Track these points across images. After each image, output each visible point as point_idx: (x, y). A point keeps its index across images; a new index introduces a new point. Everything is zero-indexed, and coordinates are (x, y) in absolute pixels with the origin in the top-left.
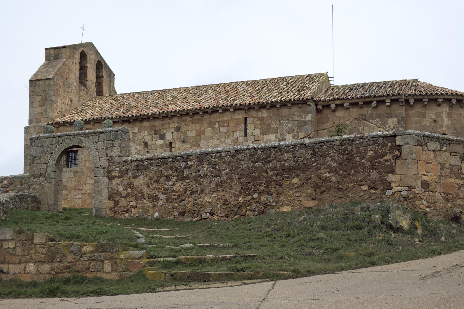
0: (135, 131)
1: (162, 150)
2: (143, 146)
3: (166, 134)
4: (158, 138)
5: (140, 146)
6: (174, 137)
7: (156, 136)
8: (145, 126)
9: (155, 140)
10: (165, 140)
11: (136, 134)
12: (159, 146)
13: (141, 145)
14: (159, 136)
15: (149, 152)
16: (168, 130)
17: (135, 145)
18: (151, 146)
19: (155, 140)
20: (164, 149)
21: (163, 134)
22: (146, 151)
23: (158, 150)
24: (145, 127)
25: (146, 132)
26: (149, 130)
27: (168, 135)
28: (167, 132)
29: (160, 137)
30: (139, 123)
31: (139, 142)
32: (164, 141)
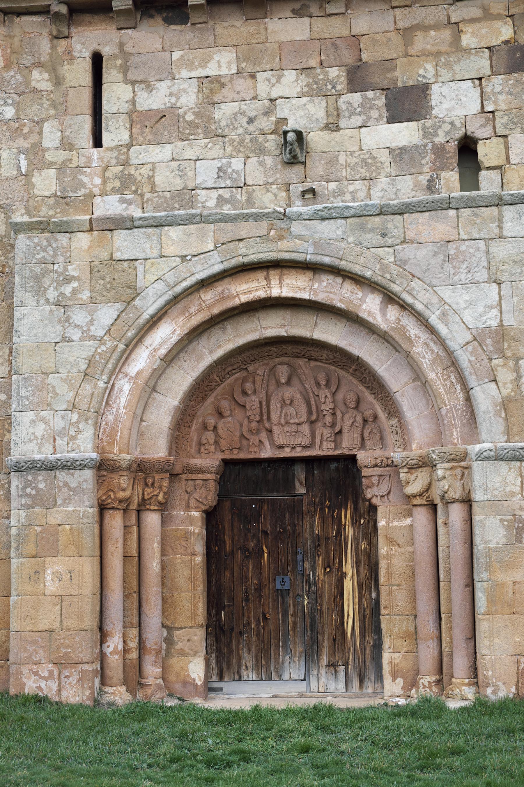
0: (211, 70)
1: (411, 184)
2: (269, 161)
3: (435, 88)
4: (375, 114)
5: (254, 160)
6: (495, 103)
7: (365, 98)
8: (284, 38)
9: (358, 120)
10: (429, 123)
11: (223, 85)
12: (385, 157)
13: (261, 151)
14: (382, 101)
15: (313, 191)
16: (448, 65)
17: (216, 151)
18: (333, 161)
19: (358, 120)
20: (423, 179)
21: (408, 90)
22: (298, 188)
23: (383, 182)
24: (281, 46)
25: (290, 76)
26: (313, 63)
27: (445, 90)
28: (437, 75)
29: (388, 107)
30: (238, 24)
31: (247, 132)
32: (424, 128)
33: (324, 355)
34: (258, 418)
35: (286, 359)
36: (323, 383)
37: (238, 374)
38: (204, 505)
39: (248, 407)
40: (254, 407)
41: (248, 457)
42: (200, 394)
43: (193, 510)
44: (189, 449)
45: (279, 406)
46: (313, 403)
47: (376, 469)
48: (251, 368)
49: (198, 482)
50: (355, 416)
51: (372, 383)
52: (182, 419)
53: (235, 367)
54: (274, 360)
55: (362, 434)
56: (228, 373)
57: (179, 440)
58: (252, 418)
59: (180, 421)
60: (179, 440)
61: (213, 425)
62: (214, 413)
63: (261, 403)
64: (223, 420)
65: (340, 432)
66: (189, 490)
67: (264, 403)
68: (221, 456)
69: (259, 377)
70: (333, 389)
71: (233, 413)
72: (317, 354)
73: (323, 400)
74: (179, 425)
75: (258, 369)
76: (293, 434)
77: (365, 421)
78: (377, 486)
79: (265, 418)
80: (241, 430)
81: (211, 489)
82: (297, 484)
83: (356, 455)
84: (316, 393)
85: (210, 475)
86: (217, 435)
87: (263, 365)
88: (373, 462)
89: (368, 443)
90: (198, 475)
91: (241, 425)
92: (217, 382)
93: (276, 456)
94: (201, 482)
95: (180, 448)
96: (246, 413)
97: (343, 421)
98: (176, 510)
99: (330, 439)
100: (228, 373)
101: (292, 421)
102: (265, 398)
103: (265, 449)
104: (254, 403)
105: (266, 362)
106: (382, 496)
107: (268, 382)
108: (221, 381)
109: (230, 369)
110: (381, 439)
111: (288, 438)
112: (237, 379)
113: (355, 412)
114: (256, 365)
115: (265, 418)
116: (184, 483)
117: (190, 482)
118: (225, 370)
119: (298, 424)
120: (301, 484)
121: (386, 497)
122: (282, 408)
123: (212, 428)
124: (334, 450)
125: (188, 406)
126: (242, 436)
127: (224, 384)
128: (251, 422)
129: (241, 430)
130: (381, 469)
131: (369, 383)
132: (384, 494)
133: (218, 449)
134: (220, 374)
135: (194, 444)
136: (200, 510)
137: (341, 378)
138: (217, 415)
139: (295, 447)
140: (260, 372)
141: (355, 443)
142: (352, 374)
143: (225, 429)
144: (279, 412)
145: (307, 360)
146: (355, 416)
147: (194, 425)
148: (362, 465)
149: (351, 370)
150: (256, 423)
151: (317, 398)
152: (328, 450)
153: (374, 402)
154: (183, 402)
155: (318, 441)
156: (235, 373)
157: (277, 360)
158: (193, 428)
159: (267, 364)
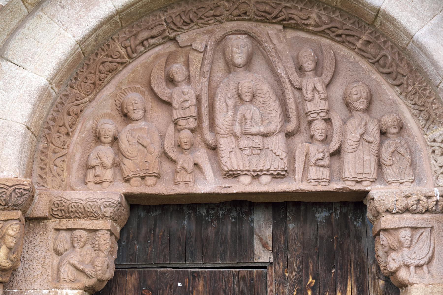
33: (314, 16)
34: (192, 123)
35: (244, 25)
36: (309, 66)
37: (160, 47)
38: (88, 276)
39: (175, 104)
40: (186, 104)
41: (172, 192)
42: (90, 76)
43: (65, 285)
44: (65, 174)
45: (231, 103)
46: (291, 101)
47: (407, 216)
48: (183, 38)
49: (77, 233)
50: (366, 125)
51: (398, 66)
52: (54, 120)
53: (155, 32)
54: (223, 26)
55: (379, 156)
56: (142, 43)
57: (46, 156)
58: (182, 122)
59: (51, 123)
60: (46, 156)
61: (111, 133)
62: (115, 113)
63: (198, 98)
64: (130, 126)
65: (337, 153)
66: (61, 248)
67: (204, 99)
68: (125, 188)
69: (196, 53)
70: (327, 76)
71: (148, 115)
72: (300, 14)
73: (309, 95)
74: (49, 129)
75: (194, 40)
76: (256, 152)
77: (383, 133)
78: (409, 247)
79: (206, 124)
80: (162, 144)
81: (103, 248)
82: (257, 246)
83: (368, 192)
84: (297, 85)
85: (101, 221)
86: (119, 152)
87: (204, 33)
88: (402, 204)
89: (389, 172)
90: (79, 221)
91: (162, 137)
92: (121, 57)
93: (223, 191)
94: (85, 233)
95: (47, 170)
96: (171, 115)
97: (344, 132)
98: (34, 285)
99: (322, 163)
100: (142, 43)
101: (254, 130)
102: (206, 90)
103: (205, 179)
104: (186, 97)
105: (209, 28)
106: (419, 266)
107: (212, 63)
108: (130, 57)
109: (145, 34)
110: (411, 165)
111: (247, 158)
112: (157, 57)
113: (366, 117)
114: (192, 33)
115: (206, 124)
116: (52, 234)
117: (64, 233)
118: (136, 35)
119: (265, 135)
120: (265, 245)
121: (425, 267)
122: (235, 107)
123: (109, 139)
124: (329, 182)
125: (67, 96)
126: (165, 154)
127: (134, 64)
128: (179, 131)
129: (162, 144)
130: (416, 216)
131: (391, 66)
132: (422, 262)
133: (119, 177)
134: (127, 43)
135: (75, 166)
136: (80, 285)
137: (339, 59)
138: (119, 118)
139: (258, 176)
140: (199, 45)
141: (367, 170)
142: (361, 53)
143: (134, 141)
144: (230, 113)
145: (281, 27)
146: (366, 125)
147: (77, 133)
148: (381, 209)
149: (359, 44)
150: (189, 132)
151: (297, 93)
152: (318, 181)
153: (399, 101)
154: (58, 85)
155: (299, 166)
156: (155, 46)
157: (230, 26)
158: (76, 137)
159: (211, 32)
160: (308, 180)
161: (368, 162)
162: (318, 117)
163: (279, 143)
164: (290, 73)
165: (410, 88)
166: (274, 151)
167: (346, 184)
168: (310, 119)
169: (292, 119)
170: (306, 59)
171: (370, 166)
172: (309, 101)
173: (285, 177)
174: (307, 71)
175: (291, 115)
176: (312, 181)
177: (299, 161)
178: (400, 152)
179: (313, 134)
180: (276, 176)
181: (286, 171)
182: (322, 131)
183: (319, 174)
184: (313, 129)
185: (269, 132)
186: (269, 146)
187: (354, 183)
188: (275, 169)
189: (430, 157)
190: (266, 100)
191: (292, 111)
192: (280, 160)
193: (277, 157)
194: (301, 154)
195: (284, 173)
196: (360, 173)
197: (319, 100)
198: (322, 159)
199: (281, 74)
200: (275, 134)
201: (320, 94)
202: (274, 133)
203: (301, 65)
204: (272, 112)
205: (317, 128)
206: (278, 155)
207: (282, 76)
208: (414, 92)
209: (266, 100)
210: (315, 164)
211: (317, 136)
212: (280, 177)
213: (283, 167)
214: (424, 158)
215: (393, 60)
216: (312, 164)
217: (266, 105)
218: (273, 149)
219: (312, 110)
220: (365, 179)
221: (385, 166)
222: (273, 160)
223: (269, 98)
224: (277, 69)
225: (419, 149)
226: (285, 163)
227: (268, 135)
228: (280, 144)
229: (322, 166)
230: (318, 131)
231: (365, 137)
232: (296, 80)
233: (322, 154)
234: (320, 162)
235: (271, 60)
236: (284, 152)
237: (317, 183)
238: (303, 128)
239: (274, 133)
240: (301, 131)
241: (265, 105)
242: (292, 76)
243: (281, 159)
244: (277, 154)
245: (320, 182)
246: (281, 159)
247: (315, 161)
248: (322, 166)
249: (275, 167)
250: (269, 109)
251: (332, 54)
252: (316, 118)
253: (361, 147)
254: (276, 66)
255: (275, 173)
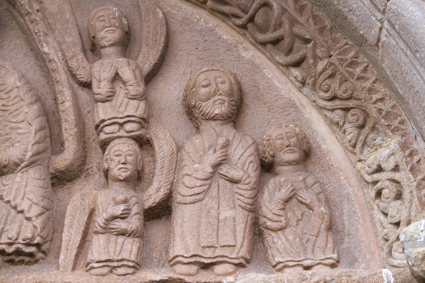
50: (227, 145)
51: (293, 22)
84: (83, 76)
99: (121, 225)
110: (330, 228)
131: (280, 25)
137: (175, 27)
141: (228, 240)
146: (227, 145)
151: (83, 94)
160: (88, 264)
161: (230, 223)
162: (122, 133)
163: (26, 186)
164: (69, 54)
165: (321, 65)
166: (13, 204)
167: (174, 271)
168: (103, 136)
169: (67, 144)
170: (102, 23)
171: (234, 231)
172: (103, 102)
173: (36, 261)
174: (104, 47)
175: (66, 135)
176: (96, 265)
177: (71, 226)
178: (304, 201)
179: (106, 166)
180: (13, 257)
181: (38, 246)
182: (126, 158)
183: (112, 250)
184: (108, 157)
185: (6, 163)
186: (4, 194)
187: (193, 269)
188: (9, 241)
189: (373, 209)
190: (11, 103)
191: (67, 127)
192: (25, 221)
193: (20, 215)
194: (78, 212)
195: (32, 249)
196: (210, 245)
197: (126, 100)
198: (123, 217)
199: (49, 54)
200: (20, 168)
201: (128, 87)
202: (17, 165)
203: (94, 37)
204: (20, 125)
205: (116, 153)
206: (22, 212)
207: (51, 58)
208: (329, 72)
209: (11, 103)
210: (105, 229)
211: (116, 169)
212: (22, 262)
213: (29, 235)
214: (359, 214)
215: (284, 10)
216: (99, 228)
217: (9, 112)
218: (11, 198)
219: (107, 118)
220: (221, 259)
221: (270, 232)
222: (8, 222)
223: (18, 99)
224: (43, 47)
225: (348, 195)
226: (35, 227)
227: (5, 170)
228: (28, 189)
229: (123, 233)
230: (117, 159)
231: (224, 170)
232: (81, 68)
233: (122, 207)
234: (117, 223)
235: (32, 31)
236: (36, 204)
237: (106, 270)
238: (95, 164)
239: (17, 165)
240: (90, 171)
241: (6, 114)
242: (74, 60)
243: (28, 219)
244: (19, 209)
245: (114, 267)
246: (28, 219)
247: (106, 220)
248: (123, 233)
249: (10, 236)
250: (15, 121)
251: (161, 15)
252: (116, 135)
253: (214, 191)
254: (40, 41)
255: (10, 250)
